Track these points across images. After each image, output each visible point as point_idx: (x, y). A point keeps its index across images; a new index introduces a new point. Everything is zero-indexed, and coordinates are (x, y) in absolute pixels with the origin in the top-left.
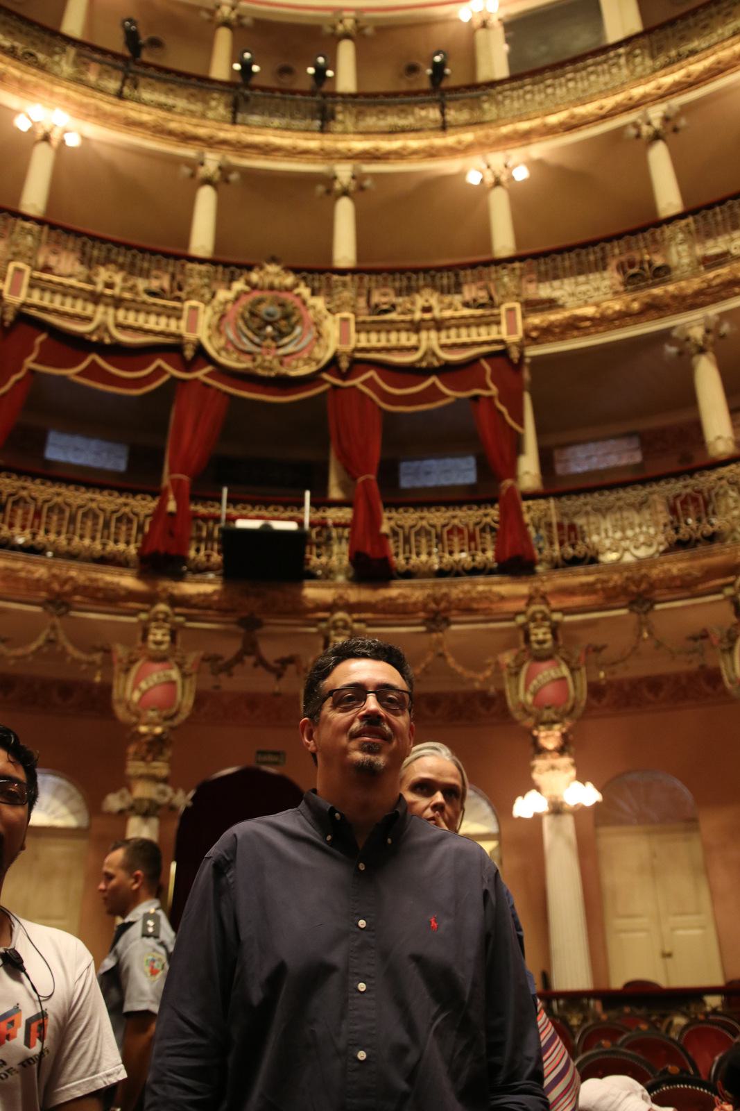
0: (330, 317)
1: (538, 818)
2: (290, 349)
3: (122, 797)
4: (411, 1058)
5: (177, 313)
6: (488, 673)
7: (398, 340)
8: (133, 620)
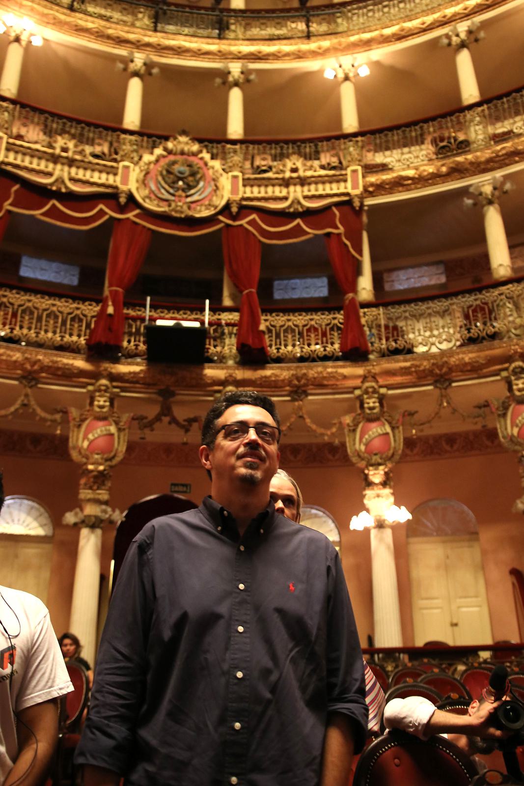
0: (224, 174)
1: (367, 531)
2: (195, 198)
3: (76, 514)
4: (274, 677)
5: (114, 171)
6: (334, 430)
7: (273, 192)
8: (84, 390)
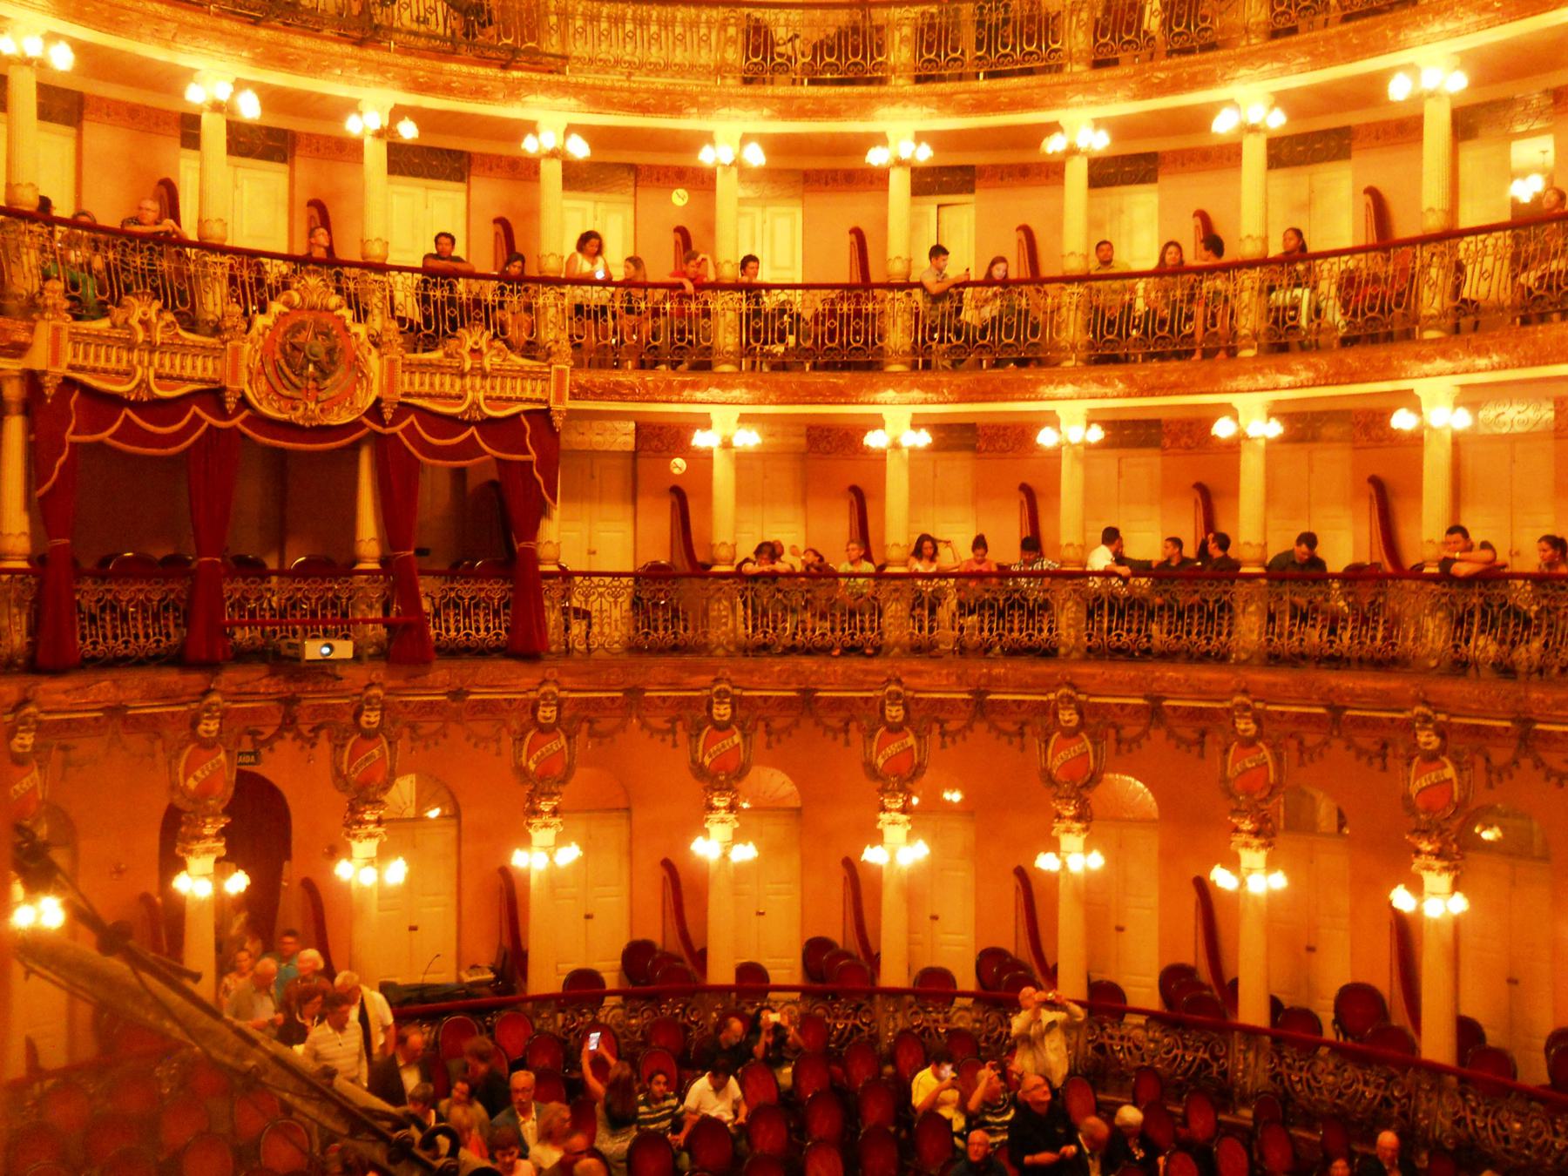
0: (374, 352)
7: (442, 385)
